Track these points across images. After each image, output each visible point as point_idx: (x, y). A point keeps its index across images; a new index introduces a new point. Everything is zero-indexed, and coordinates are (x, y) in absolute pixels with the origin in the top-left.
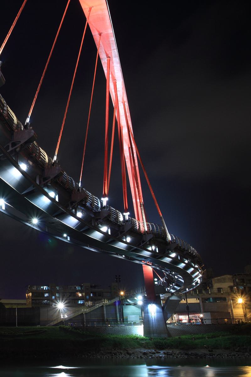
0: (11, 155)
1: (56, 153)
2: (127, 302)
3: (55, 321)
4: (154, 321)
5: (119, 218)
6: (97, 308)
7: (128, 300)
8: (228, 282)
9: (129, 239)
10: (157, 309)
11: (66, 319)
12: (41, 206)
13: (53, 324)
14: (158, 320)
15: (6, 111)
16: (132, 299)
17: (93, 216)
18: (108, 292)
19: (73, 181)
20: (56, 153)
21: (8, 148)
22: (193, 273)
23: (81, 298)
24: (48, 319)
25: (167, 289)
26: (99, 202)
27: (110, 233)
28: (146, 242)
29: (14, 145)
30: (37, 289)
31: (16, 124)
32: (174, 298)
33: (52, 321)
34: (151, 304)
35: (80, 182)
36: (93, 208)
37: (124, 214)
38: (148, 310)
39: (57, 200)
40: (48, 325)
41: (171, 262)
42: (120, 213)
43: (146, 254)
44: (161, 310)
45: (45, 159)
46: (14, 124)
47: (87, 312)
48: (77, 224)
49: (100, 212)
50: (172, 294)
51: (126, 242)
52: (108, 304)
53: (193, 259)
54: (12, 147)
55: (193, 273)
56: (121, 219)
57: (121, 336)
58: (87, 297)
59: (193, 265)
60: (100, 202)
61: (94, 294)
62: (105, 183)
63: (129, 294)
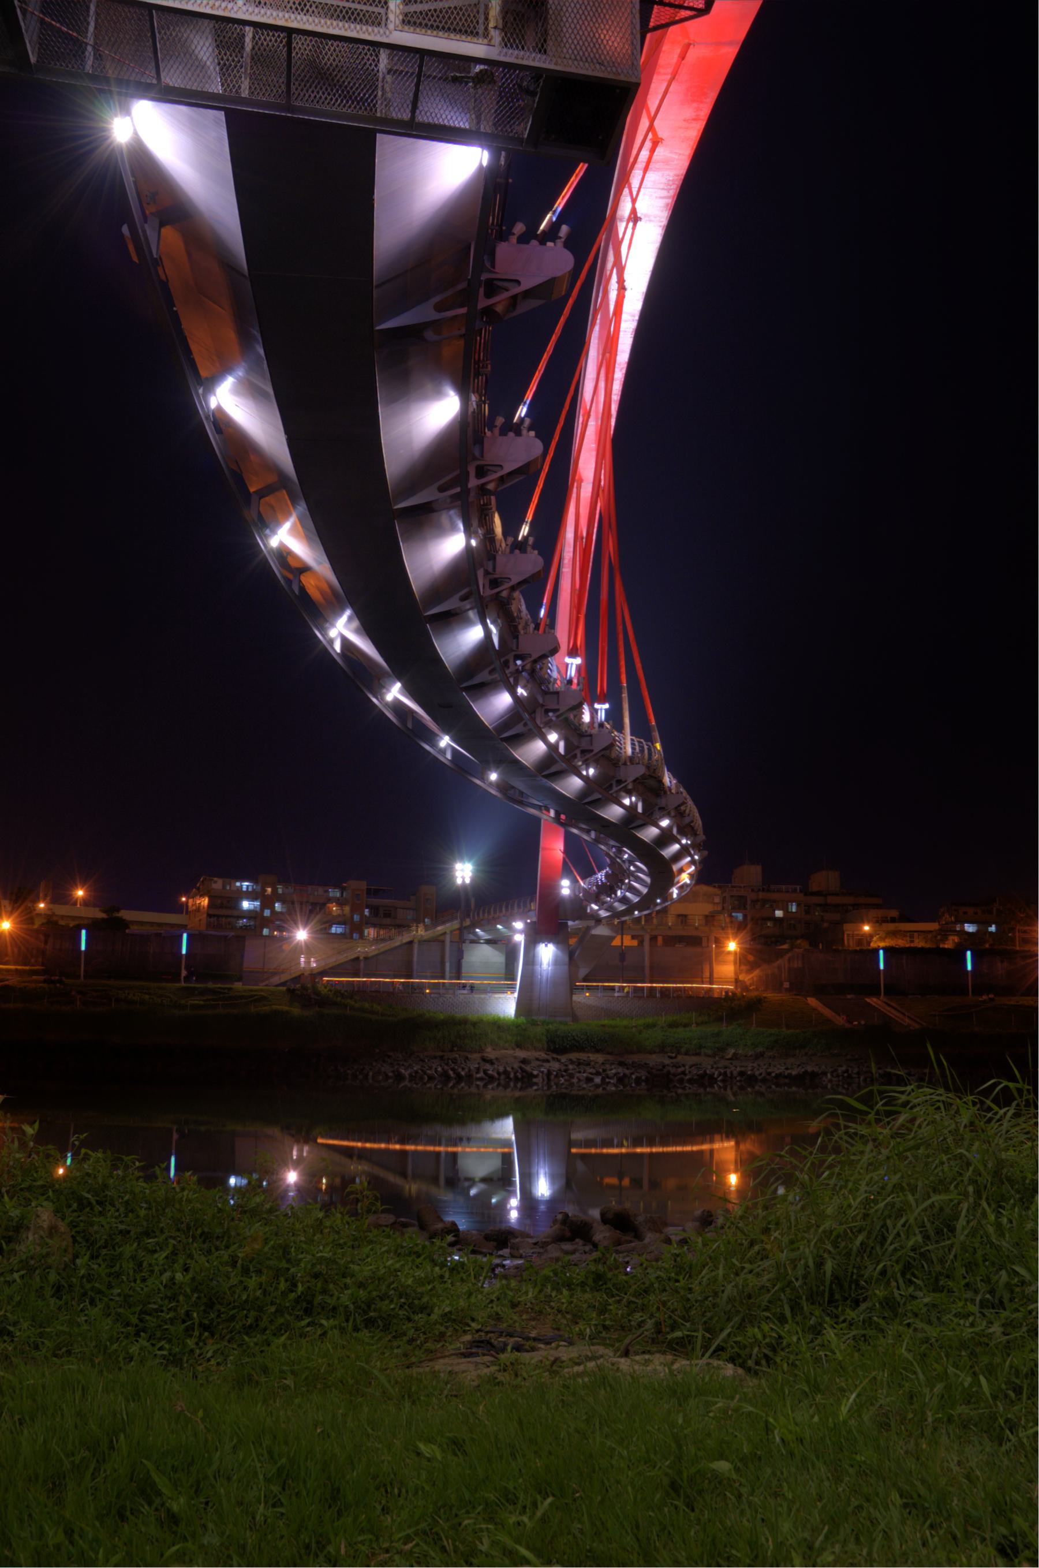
1: (529, 517)
2: (475, 934)
3: (283, 972)
7: (478, 930)
11: (312, 969)
13: (279, 982)
18: (407, 909)
20: (529, 517)
23: (341, 921)
25: (592, 909)
29: (481, 472)
30: (224, 887)
32: (601, 931)
33: (274, 974)
37: (597, 706)
40: (264, 984)
44: (566, 959)
47: (370, 955)
50: (598, 920)
52: (425, 938)
56: (586, 718)
57: (472, 1016)
59: (692, 852)
61: (375, 910)
63: (484, 913)
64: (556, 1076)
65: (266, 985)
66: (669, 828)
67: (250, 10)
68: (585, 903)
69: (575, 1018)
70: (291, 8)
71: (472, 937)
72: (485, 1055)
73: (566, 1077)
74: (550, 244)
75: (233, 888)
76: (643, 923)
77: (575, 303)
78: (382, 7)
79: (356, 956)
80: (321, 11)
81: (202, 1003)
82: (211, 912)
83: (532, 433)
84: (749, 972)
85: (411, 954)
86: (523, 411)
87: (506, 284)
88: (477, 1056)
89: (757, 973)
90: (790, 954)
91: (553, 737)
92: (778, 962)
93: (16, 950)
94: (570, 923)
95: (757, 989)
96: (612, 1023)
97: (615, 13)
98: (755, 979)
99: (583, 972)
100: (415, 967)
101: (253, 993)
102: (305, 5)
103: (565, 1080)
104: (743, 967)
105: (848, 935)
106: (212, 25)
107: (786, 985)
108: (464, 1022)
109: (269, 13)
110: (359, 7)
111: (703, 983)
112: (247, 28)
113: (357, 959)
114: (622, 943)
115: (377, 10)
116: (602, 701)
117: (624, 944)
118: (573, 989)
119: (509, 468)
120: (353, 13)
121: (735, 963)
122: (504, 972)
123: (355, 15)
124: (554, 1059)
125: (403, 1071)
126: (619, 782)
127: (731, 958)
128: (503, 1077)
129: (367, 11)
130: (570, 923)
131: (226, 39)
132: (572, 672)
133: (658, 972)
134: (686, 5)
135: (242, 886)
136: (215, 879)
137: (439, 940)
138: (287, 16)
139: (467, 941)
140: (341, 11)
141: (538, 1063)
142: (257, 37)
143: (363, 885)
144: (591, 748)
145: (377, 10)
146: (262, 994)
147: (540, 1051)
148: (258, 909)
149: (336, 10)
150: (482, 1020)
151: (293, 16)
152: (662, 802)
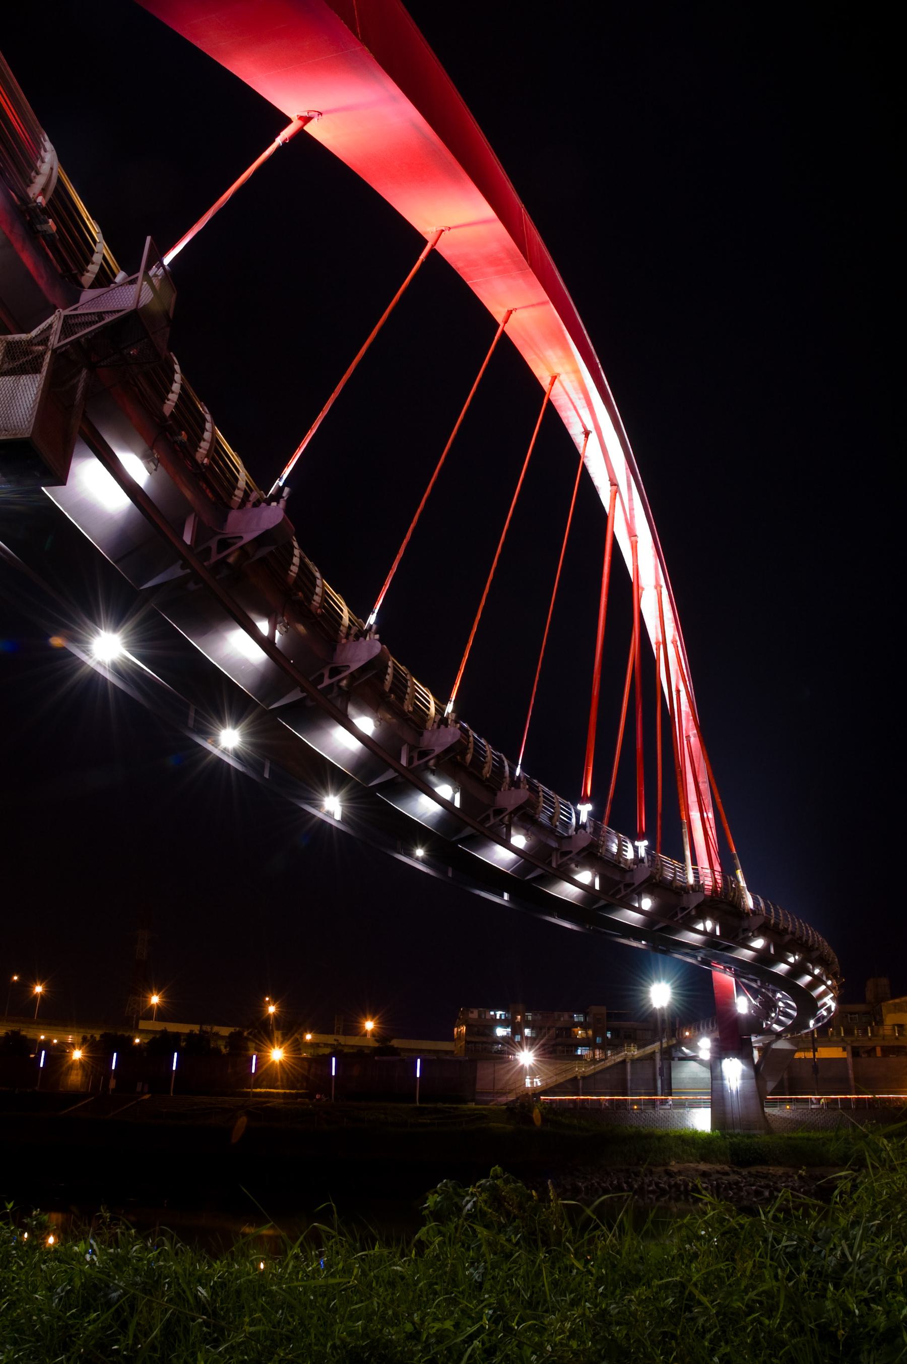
0: (329, 697)
4: (735, 1098)
5: (624, 853)
9: (647, 903)
10: (743, 1071)
12: (421, 816)
15: (319, 596)
17: (554, 845)
19: (506, 763)
21: (320, 679)
22: (813, 985)
26: (574, 815)
27: (597, 887)
29: (335, 672)
30: (480, 1016)
31: (346, 627)
32: (782, 1045)
34: (728, 1058)
35: (519, 766)
36: (556, 826)
37: (637, 843)
38: (721, 1071)
39: (457, 804)
41: (755, 959)
42: (628, 842)
43: (692, 938)
44: (753, 1073)
45: (428, 709)
46: (343, 626)
47: (586, 1075)
48: (517, 862)
49: (570, 837)
51: (639, 910)
53: (811, 955)
54: (331, 677)
55: (813, 985)
57: (659, 1132)
60: (576, 813)
62: (587, 769)
64: (725, 1189)
65: (496, 1104)
66: (766, 949)
69: (770, 1131)
71: (681, 1055)
72: (670, 1168)
73: (735, 1191)
74: (274, 504)
75: (488, 1017)
76: (843, 1035)
79: (574, 1075)
81: (429, 1121)
82: (469, 1039)
83: (377, 636)
85: (625, 1073)
86: (372, 619)
87: (234, 540)
88: (660, 1169)
91: (585, 876)
93: (285, 1076)
96: (806, 1134)
99: (771, 1085)
100: (629, 1085)
101: (476, 1112)
103: (734, 1193)
108: (650, 1136)
113: (576, 1078)
114: (814, 1055)
116: (640, 839)
117: (817, 1057)
119: (354, 666)
124: (734, 1172)
125: (580, 1184)
126: (684, 909)
128: (673, 1190)
132: (584, 818)
133: (865, 1083)
135: (495, 1015)
136: (472, 1010)
137: (651, 1057)
139: (676, 1059)
141: (720, 1176)
143: (603, 1010)
144: (632, 882)
146: (484, 1112)
147: (724, 1164)
148: (510, 1035)
150: (667, 1135)
152: (745, 924)
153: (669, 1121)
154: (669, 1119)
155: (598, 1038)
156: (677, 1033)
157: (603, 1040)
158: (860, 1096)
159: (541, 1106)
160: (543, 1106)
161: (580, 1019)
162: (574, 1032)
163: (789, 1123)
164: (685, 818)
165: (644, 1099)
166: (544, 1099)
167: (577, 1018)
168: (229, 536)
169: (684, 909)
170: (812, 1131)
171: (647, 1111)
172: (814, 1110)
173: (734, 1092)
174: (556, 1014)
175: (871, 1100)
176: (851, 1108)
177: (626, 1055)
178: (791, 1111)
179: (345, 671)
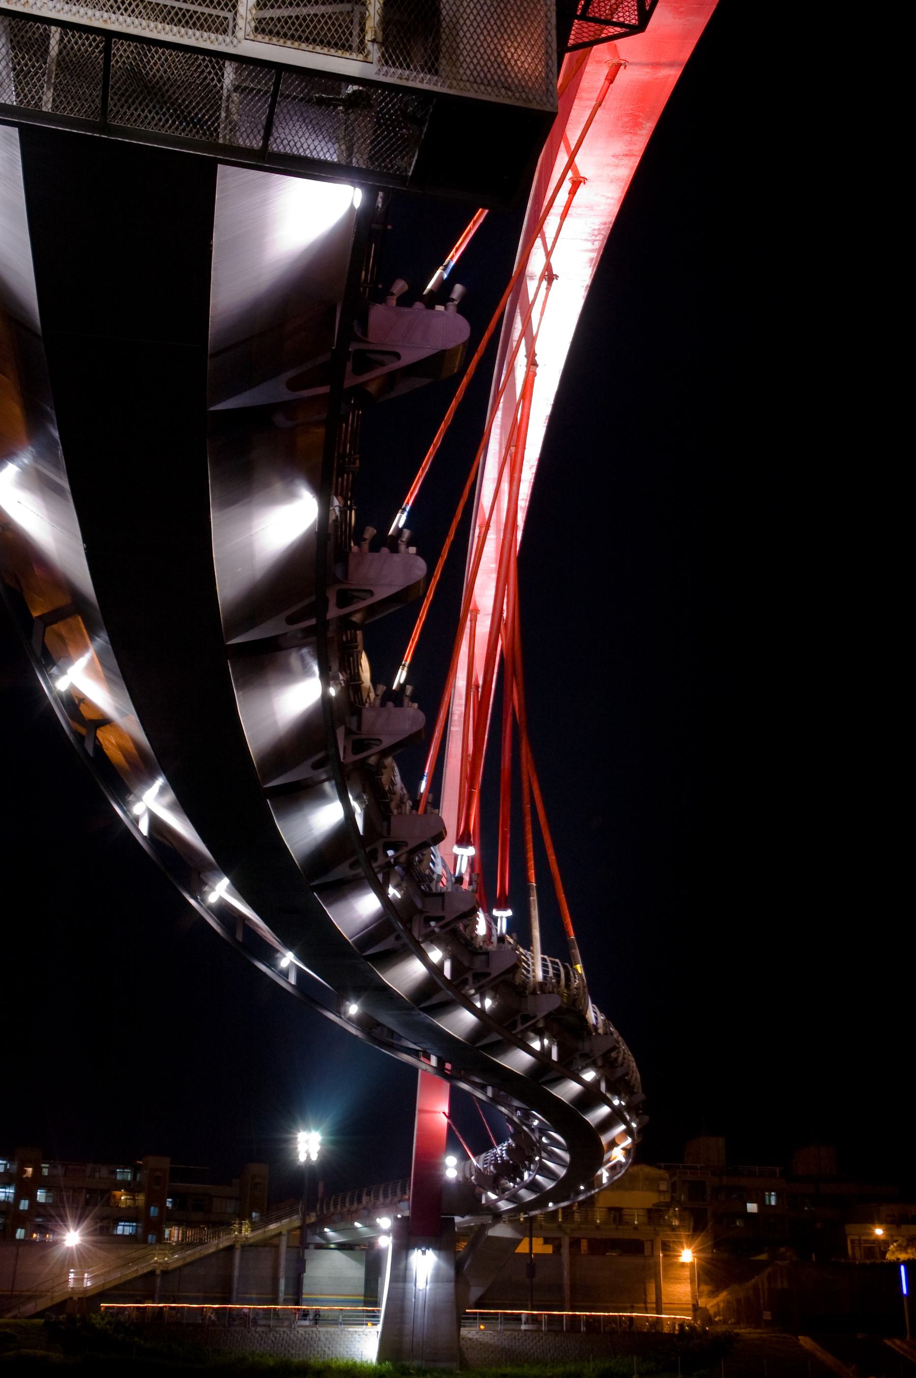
1: (407, 659)
2: (323, 1235)
3: (41, 1297)
6: (213, 1254)
7: (326, 1230)
8: (642, 1190)
11: (86, 1290)
14: (435, 1311)
16: (342, 1225)
20: (407, 659)
23: (128, 1216)
24: (12, 1291)
25: (487, 1198)
28: (533, 1021)
29: (345, 599)
32: (501, 1231)
33: (30, 1298)
34: (419, 1248)
37: (495, 913)
44: (451, 1273)
50: (497, 1216)
52: (251, 1241)
56: (481, 929)
57: (315, 1361)
58: (154, 1211)
59: (628, 1118)
61: (180, 1200)
63: (335, 1205)
65: (15, 1317)
66: (596, 1083)
67: (59, 6)
68: (479, 1189)
70: (112, 7)
71: (318, 1239)
74: (439, 308)
77: (453, 543)
78: (230, 11)
79: (150, 1269)
80: (150, 12)
83: (413, 550)
84: (713, 1294)
86: (401, 520)
87: (379, 357)
89: (723, 1295)
90: (770, 1269)
92: (753, 1281)
94: (458, 1219)
95: (725, 1322)
97: (526, 41)
98: (722, 1305)
99: (475, 1293)
100: (235, 1286)
102: (130, 4)
104: (705, 1288)
105: (853, 1241)
106: (6, 23)
107: (767, 1315)
109: (82, 11)
110: (200, 9)
111: (646, 1310)
112: (53, 28)
113: (152, 1273)
114: (531, 1249)
115: (222, 14)
117: (534, 1251)
118: (461, 1318)
119: (381, 594)
120: (191, 17)
121: (692, 1282)
122: (362, 1290)
123: (194, 19)
126: (526, 1018)
127: (686, 1273)
129: (211, 15)
130: (458, 1219)
131: (25, 40)
132: (463, 867)
134: (614, 20)
137: (270, 1244)
138: (106, 15)
139: (312, 1246)
140: (176, 14)
142: (66, 39)
143: (165, 1163)
145: (222, 14)
146: (8, 1330)
148: (11, 1200)
149: (169, 13)
151: (113, 17)
152: (586, 1046)
153: (311, 1346)
154: (312, 1343)
155: (152, 1208)
156: (318, 1206)
157: (161, 1213)
158: (593, 1313)
159: (103, 1319)
160: (106, 1320)
161: (125, 1177)
162: (115, 1196)
163: (492, 1352)
164: (533, 880)
165: (566, 1314)
166: (107, 1308)
167: (124, 1175)
168: (371, 347)
169: (526, 1018)
170: (526, 1365)
171: (277, 1329)
172: (529, 1333)
173: (421, 1302)
174: (90, 1167)
175: (591, 1320)
176: (579, 1331)
177: (236, 1237)
178: (495, 1334)
179: (364, 600)
